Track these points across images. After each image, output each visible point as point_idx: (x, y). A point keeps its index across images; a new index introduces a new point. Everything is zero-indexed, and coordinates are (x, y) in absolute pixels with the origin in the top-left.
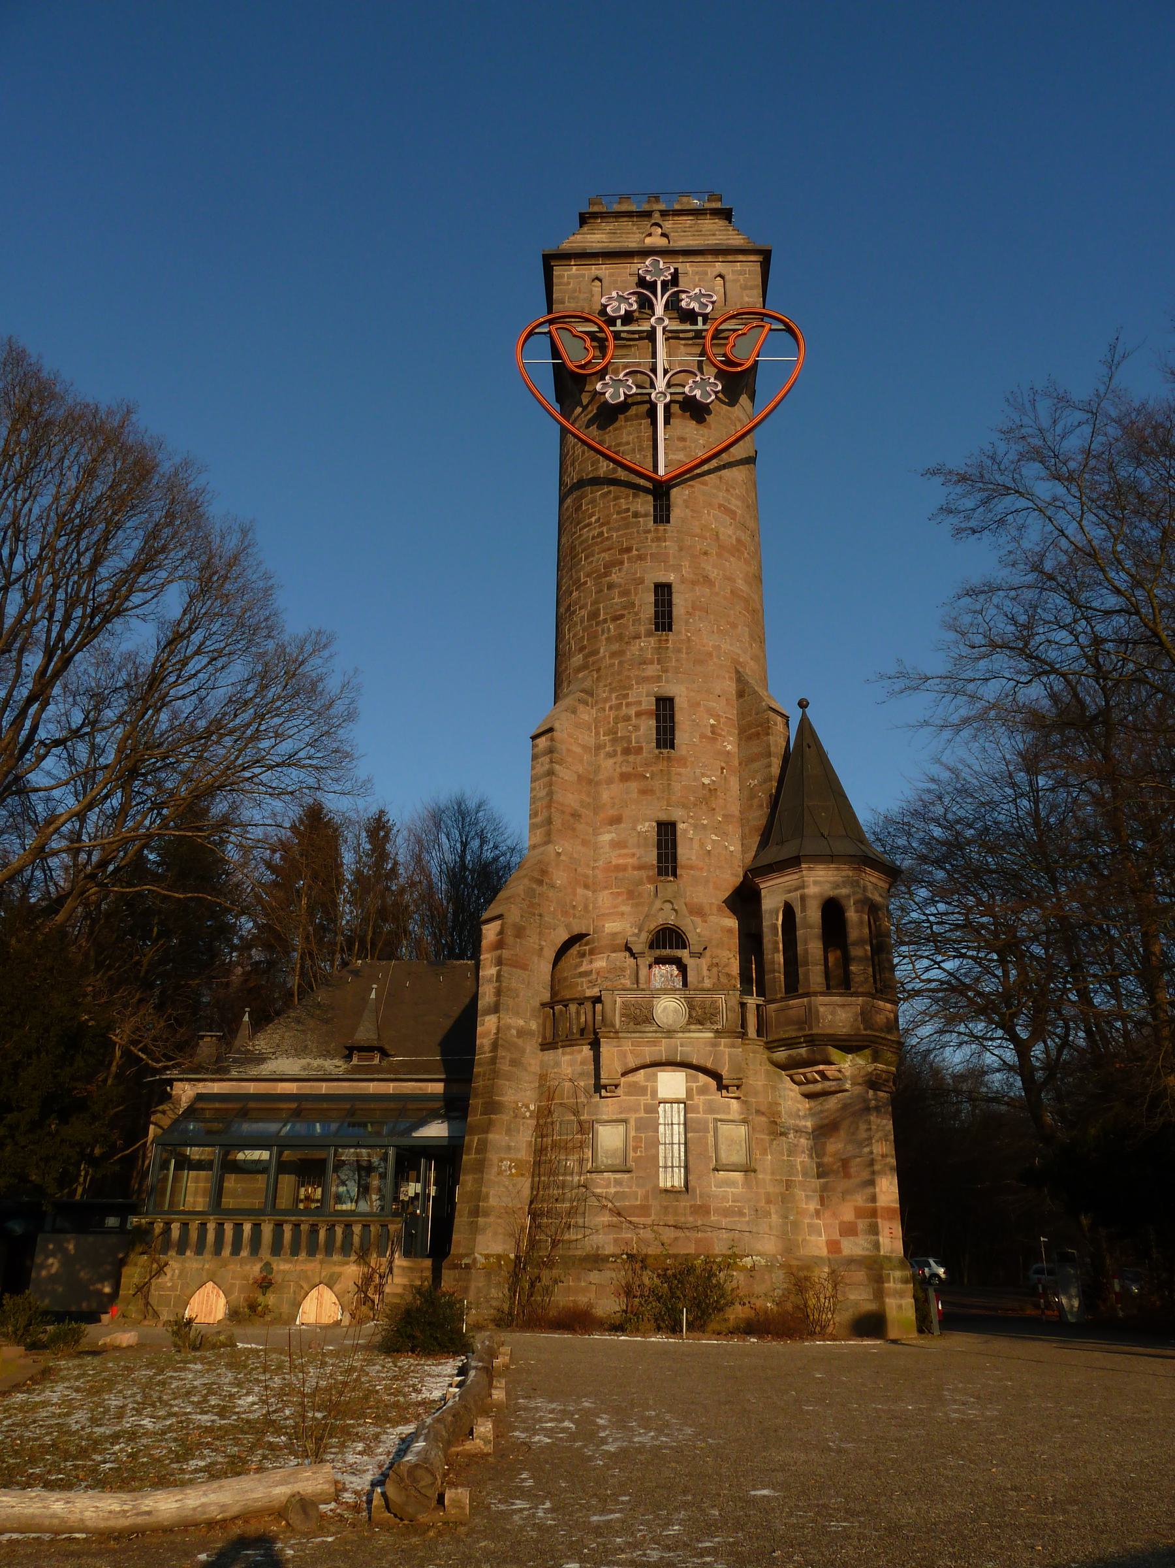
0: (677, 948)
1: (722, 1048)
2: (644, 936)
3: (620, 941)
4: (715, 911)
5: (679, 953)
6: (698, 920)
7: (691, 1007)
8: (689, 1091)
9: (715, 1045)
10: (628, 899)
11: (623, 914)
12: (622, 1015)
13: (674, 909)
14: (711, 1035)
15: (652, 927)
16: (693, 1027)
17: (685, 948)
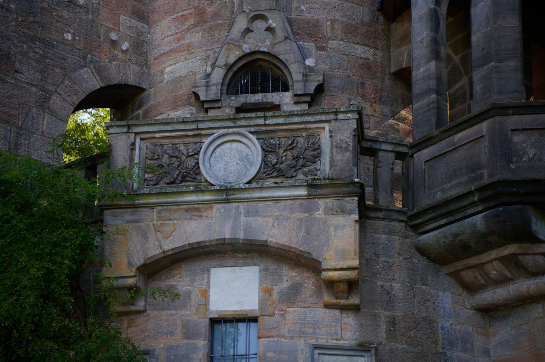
0: (275, 90)
1: (319, 214)
2: (218, 75)
3: (184, 89)
4: (339, 33)
5: (273, 97)
6: (310, 46)
7: (266, 151)
8: (266, 292)
9: (310, 210)
10: (195, 25)
11: (189, 48)
12: (146, 169)
13: (269, 29)
14: (303, 192)
15: (232, 59)
16: (268, 183)
17: (286, 88)
